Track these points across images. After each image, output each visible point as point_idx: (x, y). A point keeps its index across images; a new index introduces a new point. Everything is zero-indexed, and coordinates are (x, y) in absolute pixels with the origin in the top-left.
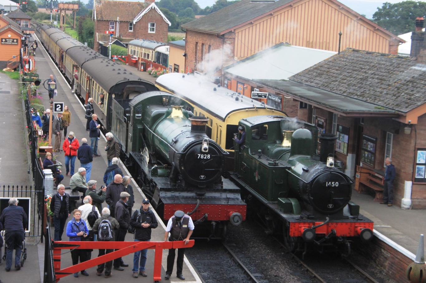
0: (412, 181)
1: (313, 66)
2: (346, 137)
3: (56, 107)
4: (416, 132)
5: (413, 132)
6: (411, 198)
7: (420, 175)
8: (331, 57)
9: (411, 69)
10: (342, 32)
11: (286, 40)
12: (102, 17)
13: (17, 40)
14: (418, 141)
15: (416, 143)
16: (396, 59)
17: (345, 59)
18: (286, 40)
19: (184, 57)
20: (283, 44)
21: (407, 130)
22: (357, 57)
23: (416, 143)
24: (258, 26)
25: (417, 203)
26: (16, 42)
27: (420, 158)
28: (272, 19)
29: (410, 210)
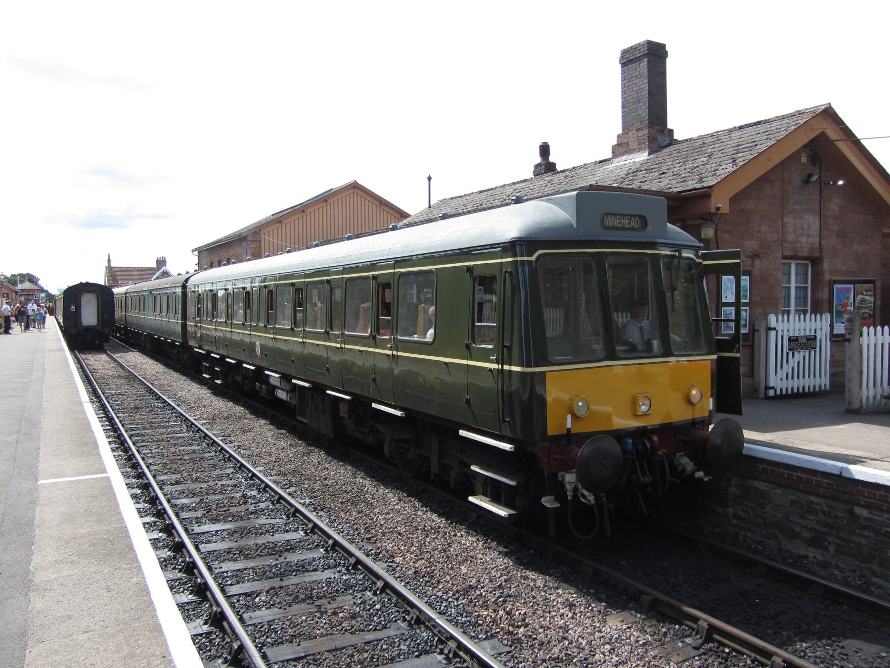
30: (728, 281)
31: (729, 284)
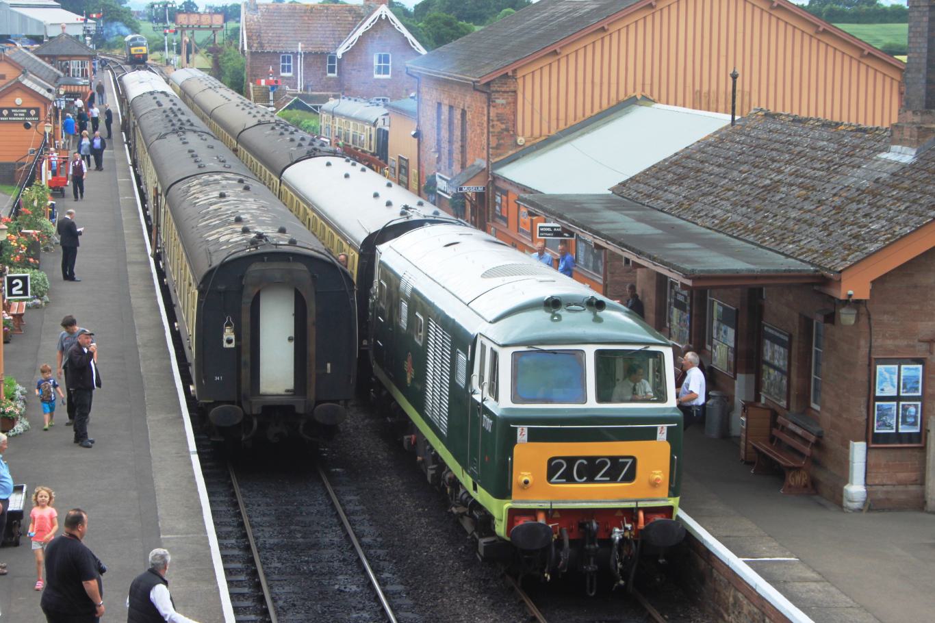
0: (867, 441)
1: (671, 157)
2: (731, 333)
3: (11, 286)
4: (869, 319)
5: (864, 319)
6: (866, 484)
7: (885, 425)
8: (715, 133)
9: (876, 161)
10: (739, 71)
11: (643, 90)
12: (261, 45)
13: (37, 110)
14: (877, 342)
15: (871, 347)
16: (853, 134)
17: (743, 138)
18: (643, 90)
19: (416, 140)
20: (637, 99)
21: (847, 317)
22: (770, 131)
23: (871, 347)
24: (572, 59)
25: (880, 496)
26: (35, 116)
27: (884, 384)
28: (607, 40)
29: (864, 512)
30: (885, 371)
31: (887, 376)
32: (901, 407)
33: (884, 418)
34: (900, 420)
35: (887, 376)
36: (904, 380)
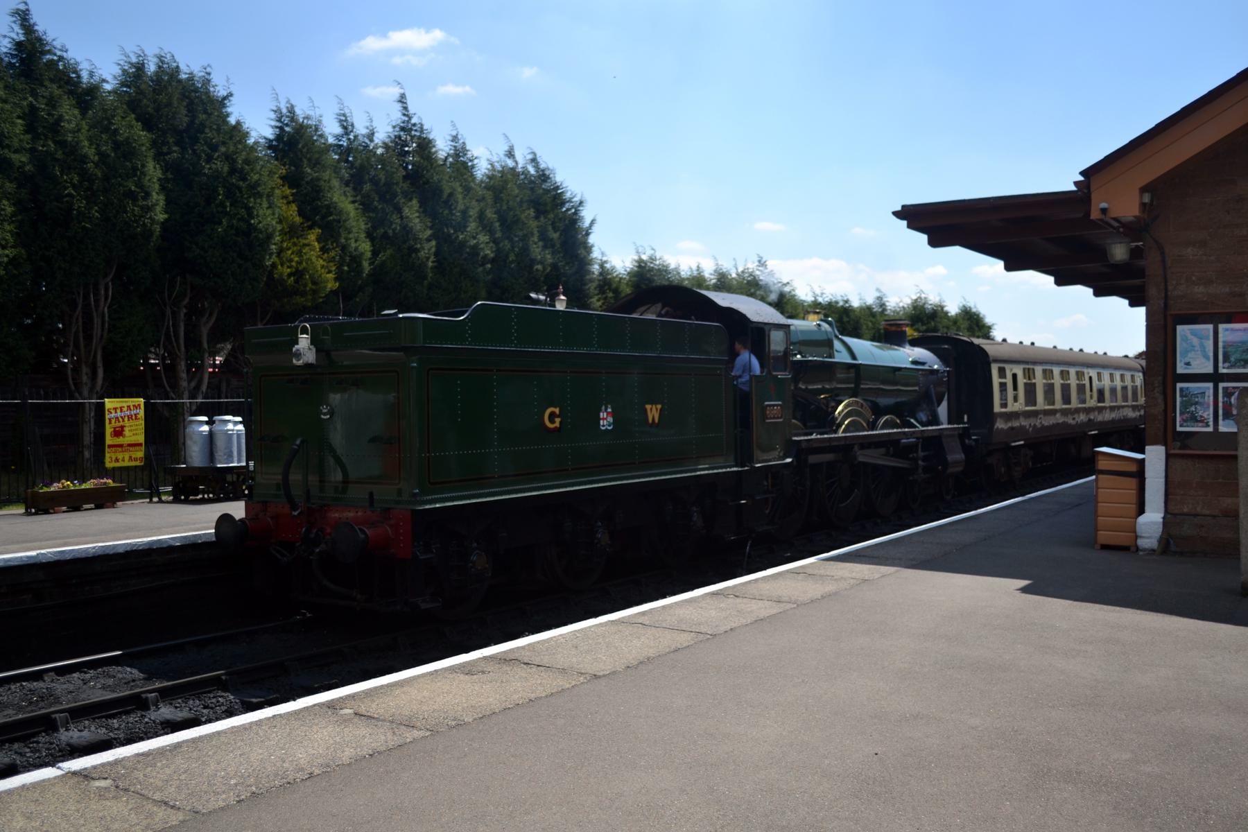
0: (1165, 444)
4: (1163, 253)
7: (1194, 419)
15: (1166, 297)
23: (1166, 297)
31: (1195, 341)
32: (1220, 391)
33: (1193, 409)
34: (1221, 412)
35: (1195, 341)
36: (1224, 347)
